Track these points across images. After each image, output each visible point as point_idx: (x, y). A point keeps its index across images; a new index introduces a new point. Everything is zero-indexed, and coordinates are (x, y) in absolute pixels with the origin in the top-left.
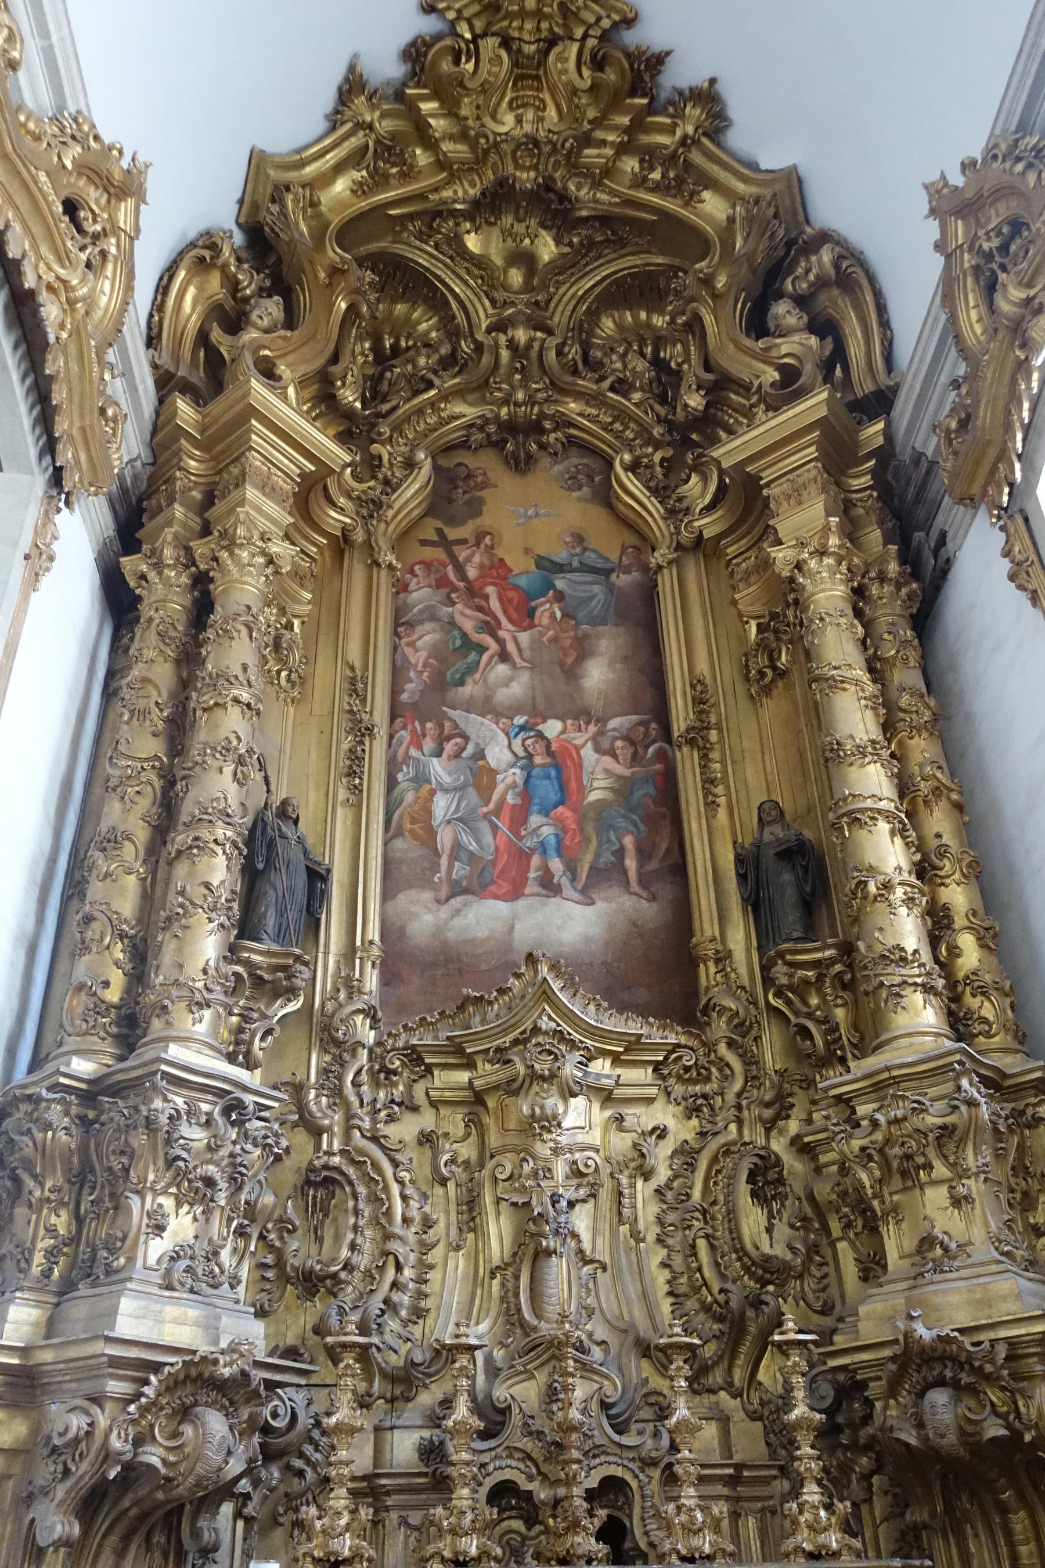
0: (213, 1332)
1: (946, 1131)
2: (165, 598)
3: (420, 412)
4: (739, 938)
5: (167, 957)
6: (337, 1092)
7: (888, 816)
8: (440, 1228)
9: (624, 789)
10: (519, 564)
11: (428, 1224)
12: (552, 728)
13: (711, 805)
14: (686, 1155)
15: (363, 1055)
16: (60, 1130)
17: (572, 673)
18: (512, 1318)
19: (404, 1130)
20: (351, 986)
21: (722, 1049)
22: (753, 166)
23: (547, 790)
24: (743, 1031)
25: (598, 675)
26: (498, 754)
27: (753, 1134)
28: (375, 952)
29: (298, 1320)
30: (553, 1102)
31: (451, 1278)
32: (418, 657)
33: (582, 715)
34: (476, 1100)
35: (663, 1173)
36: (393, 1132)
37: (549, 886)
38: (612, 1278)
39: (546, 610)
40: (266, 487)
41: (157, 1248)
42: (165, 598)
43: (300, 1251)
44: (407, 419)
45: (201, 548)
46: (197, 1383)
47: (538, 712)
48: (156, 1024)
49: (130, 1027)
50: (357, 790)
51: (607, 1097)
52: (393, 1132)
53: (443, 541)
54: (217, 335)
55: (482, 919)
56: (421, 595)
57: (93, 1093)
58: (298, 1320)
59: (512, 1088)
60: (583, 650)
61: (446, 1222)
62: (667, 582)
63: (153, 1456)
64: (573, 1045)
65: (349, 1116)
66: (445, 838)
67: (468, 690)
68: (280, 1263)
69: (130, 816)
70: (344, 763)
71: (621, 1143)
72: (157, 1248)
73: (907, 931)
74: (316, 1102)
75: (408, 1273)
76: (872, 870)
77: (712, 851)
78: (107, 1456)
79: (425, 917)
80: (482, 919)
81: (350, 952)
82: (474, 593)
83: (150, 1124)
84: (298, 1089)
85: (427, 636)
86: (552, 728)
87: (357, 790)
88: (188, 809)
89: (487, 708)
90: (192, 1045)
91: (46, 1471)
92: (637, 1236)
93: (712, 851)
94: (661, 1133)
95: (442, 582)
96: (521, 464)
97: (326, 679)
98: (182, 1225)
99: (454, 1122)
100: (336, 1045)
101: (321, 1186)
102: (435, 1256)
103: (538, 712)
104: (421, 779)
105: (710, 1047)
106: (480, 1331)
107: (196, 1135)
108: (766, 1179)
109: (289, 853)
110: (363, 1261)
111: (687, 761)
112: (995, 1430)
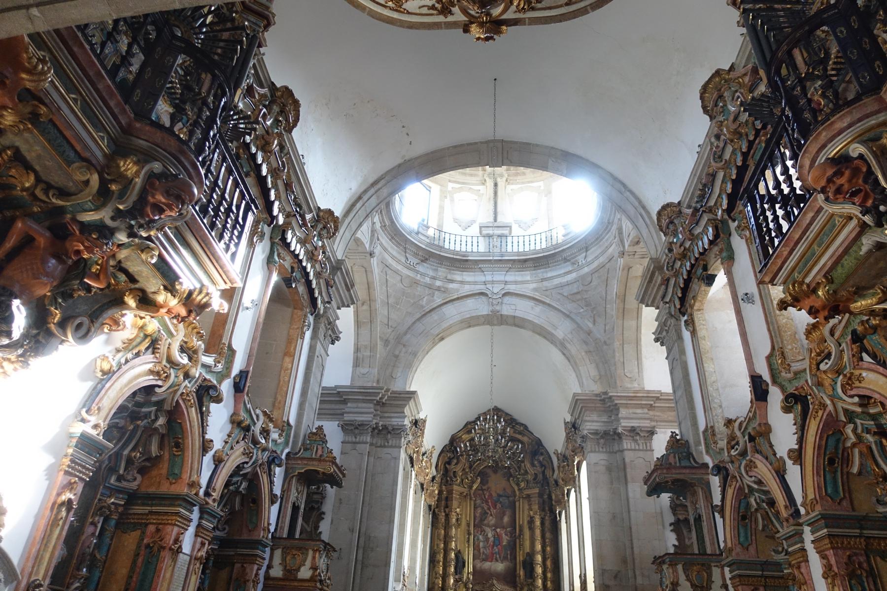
2: (442, 517)
4: (522, 573)
9: (509, 542)
10: (494, 494)
12: (498, 530)
17: (502, 519)
20: (468, 578)
23: (497, 542)
25: (506, 519)
26: (490, 535)
32: (478, 515)
33: (503, 528)
37: (497, 561)
39: (499, 506)
42: (442, 517)
45: (447, 510)
47: (496, 526)
53: (482, 490)
55: (487, 565)
56: (478, 502)
60: (504, 514)
62: (517, 504)
66: (482, 550)
67: (486, 522)
69: (440, 557)
77: (520, 558)
79: (479, 565)
80: (487, 565)
82: (487, 502)
85: (479, 511)
86: (498, 530)
89: (489, 526)
93: (520, 558)
95: (482, 499)
96: (495, 472)
97: (464, 523)
103: (496, 526)
104: (478, 539)
109: (460, 559)
111: (518, 541)
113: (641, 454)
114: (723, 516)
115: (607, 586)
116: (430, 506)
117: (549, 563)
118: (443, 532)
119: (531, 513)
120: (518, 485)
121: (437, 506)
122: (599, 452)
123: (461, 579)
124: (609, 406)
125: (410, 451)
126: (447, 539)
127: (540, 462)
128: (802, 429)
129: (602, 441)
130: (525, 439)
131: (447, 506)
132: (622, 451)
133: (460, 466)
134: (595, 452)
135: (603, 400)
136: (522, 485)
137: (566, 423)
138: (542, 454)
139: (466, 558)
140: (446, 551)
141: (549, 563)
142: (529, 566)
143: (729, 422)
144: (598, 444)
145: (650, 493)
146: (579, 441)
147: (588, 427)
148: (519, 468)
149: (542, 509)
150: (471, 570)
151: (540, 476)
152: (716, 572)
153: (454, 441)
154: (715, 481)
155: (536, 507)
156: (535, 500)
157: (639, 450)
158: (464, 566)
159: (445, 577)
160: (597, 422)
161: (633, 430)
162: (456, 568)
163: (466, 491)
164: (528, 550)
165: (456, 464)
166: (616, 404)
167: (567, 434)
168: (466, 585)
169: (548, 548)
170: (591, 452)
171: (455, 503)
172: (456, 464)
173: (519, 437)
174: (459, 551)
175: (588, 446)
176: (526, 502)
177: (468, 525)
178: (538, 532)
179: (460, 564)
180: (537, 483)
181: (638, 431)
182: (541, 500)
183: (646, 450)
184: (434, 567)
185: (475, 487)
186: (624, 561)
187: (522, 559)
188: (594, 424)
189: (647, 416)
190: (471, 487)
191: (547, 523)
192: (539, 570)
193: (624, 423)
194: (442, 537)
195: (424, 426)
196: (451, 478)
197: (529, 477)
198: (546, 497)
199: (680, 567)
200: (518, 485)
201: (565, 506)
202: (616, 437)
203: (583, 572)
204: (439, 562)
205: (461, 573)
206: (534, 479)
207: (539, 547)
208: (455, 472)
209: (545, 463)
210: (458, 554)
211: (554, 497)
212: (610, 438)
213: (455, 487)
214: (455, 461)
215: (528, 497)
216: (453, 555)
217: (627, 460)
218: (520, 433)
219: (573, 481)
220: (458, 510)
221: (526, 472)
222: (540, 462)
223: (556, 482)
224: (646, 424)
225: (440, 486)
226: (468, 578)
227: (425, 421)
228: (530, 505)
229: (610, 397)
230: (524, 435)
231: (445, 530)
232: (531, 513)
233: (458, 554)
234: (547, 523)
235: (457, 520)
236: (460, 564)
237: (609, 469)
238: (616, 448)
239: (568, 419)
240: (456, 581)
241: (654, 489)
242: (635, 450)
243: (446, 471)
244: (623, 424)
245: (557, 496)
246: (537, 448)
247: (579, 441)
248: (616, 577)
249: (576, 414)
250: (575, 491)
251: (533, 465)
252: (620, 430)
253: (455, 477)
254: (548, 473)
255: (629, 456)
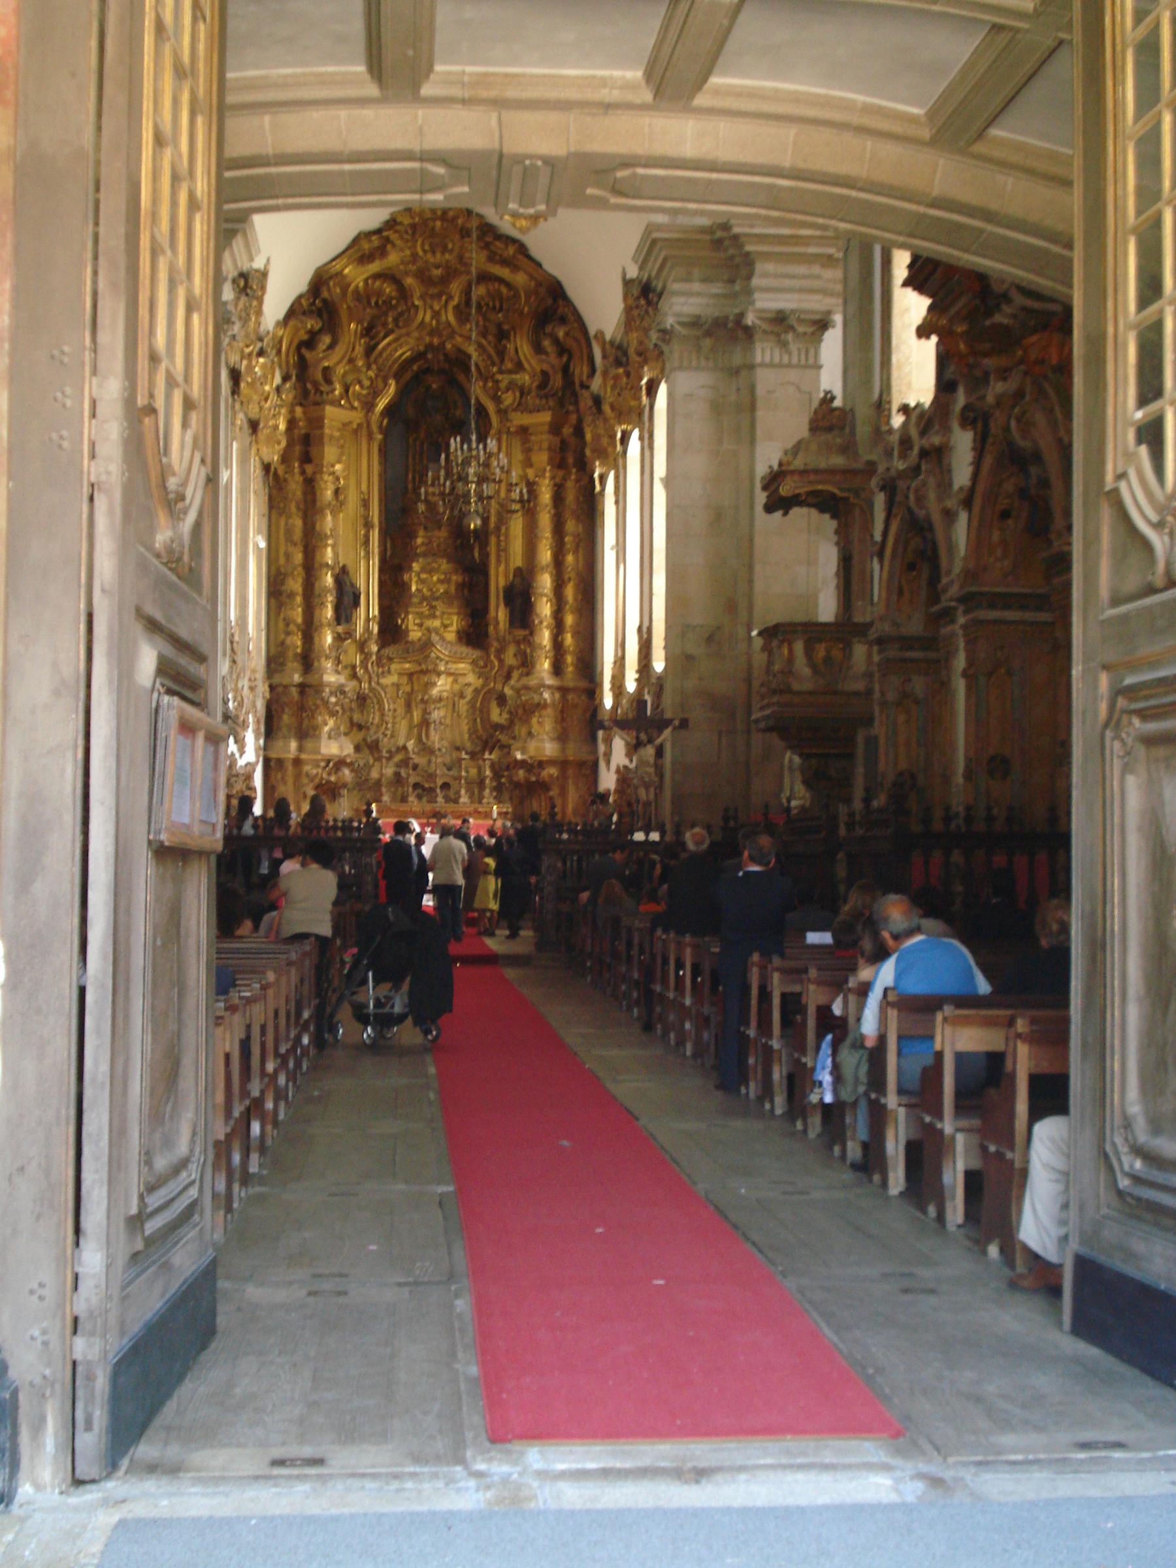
0: (341, 747)
1: (538, 704)
3: (389, 344)
5: (316, 639)
6: (366, 669)
7: (546, 595)
8: (399, 711)
11: (395, 710)
13: (498, 561)
14: (477, 691)
15: (374, 657)
16: (294, 691)
18: (420, 740)
19: (388, 681)
21: (492, 657)
22: (539, 265)
24: (500, 652)
27: (499, 687)
28: (377, 619)
29: (359, 736)
30: (434, 678)
31: (403, 727)
34: (411, 675)
35: (468, 698)
36: (383, 681)
38: (448, 730)
40: (331, 437)
41: (326, 729)
42: (295, 486)
43: (357, 717)
44: (384, 349)
45: (309, 469)
46: (340, 763)
48: (316, 664)
49: (307, 661)
50: (368, 553)
51: (449, 674)
52: (383, 681)
54: (304, 351)
57: (302, 687)
58: (359, 736)
59: (422, 672)
61: (401, 710)
63: (333, 779)
64: (441, 660)
65: (370, 678)
68: (351, 720)
69: (295, 585)
70: (363, 540)
71: (457, 687)
72: (326, 729)
73: (545, 637)
74: (360, 672)
75: (390, 726)
76: (537, 615)
78: (322, 778)
81: (368, 620)
83: (322, 699)
84: (354, 667)
87: (368, 553)
88: (317, 592)
90: (331, 677)
91: (305, 780)
92: (459, 716)
93: (498, 579)
94: (468, 685)
97: (352, 499)
98: (331, 722)
99: (405, 680)
100: (366, 656)
101: (362, 699)
102: (398, 719)
105: (488, 656)
106: (411, 745)
107: (333, 700)
108: (502, 700)
109: (348, 588)
110: (377, 720)
112: (533, 779)
113: (793, 375)
114: (881, 562)
115: (689, 658)
116: (267, 468)
117: (569, 592)
118: (298, 523)
119: (531, 473)
120: (497, 399)
121: (285, 458)
122: (697, 369)
123: (349, 634)
124: (732, 258)
125: (234, 358)
126: (311, 542)
127: (556, 341)
128: (977, 464)
129: (707, 343)
130: (520, 279)
131: (306, 459)
132: (751, 367)
133: (340, 350)
134: (689, 368)
135: (720, 241)
136: (508, 399)
137: (627, 283)
138: (563, 320)
139: (361, 584)
140: (311, 568)
141: (569, 592)
142: (520, 599)
143: (905, 409)
144: (699, 349)
145: (769, 508)
146: (654, 336)
147: (677, 308)
148: (501, 353)
149: (559, 464)
150: (375, 611)
151: (557, 381)
152: (860, 651)
153: (319, 281)
154: (880, 500)
155: (541, 458)
156: (543, 439)
157: (789, 366)
158: (356, 604)
159: (309, 630)
160: (698, 294)
161: (780, 320)
162: (337, 609)
163: (356, 417)
164: (517, 560)
165: (331, 347)
166: (748, 254)
167: (628, 310)
168: (362, 646)
169: (570, 558)
170: (680, 368)
171: (330, 452)
172: (331, 347)
173: (504, 272)
174: (344, 570)
175: (675, 352)
176: (517, 444)
177: (366, 504)
178: (545, 520)
179: (347, 600)
180: (546, 397)
181: (792, 321)
182: (557, 440)
183: (806, 367)
184: (280, 606)
185: (381, 404)
186: (731, 607)
187: (502, 582)
188: (692, 300)
189: (816, 284)
190: (369, 406)
191: (570, 497)
192: (545, 609)
193: (766, 303)
194: (298, 533)
195: (263, 288)
196: (316, 385)
197: (525, 378)
198: (567, 431)
199: (799, 647)
200: (497, 399)
201: (618, 463)
202: (740, 333)
203: (646, 624)
204: (292, 595)
205: (348, 619)
206: (543, 385)
207: (545, 555)
208: (326, 369)
209: (571, 343)
210: (343, 578)
211: (588, 437)
212: (727, 333)
213: (329, 410)
214: (327, 340)
215: (524, 431)
216: (329, 580)
217: (760, 391)
218: (505, 262)
219: (641, 417)
220: (338, 467)
221: (519, 367)
222: (556, 341)
223: (597, 401)
224: (815, 304)
225: (292, 411)
226: (367, 629)
227: (264, 274)
228: (527, 451)
229: (736, 237)
230: (515, 268)
231: (305, 518)
232: (531, 473)
233: (343, 578)
234: (570, 497)
235: (337, 492)
236: (347, 600)
237: (717, 408)
238: (737, 359)
239: (633, 272)
240: (339, 638)
241: (778, 504)
242: (780, 366)
243: (303, 366)
244: (759, 304)
245: (597, 438)
246: (553, 305)
247: (654, 336)
248: (710, 639)
249: (653, 267)
250: (641, 438)
251: (538, 349)
252: (750, 319)
253: (328, 381)
254: (580, 370)
255: (765, 379)
